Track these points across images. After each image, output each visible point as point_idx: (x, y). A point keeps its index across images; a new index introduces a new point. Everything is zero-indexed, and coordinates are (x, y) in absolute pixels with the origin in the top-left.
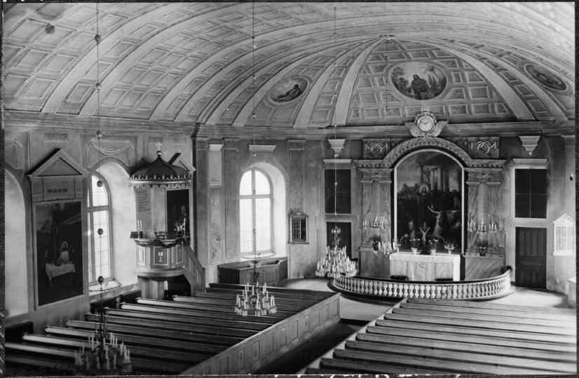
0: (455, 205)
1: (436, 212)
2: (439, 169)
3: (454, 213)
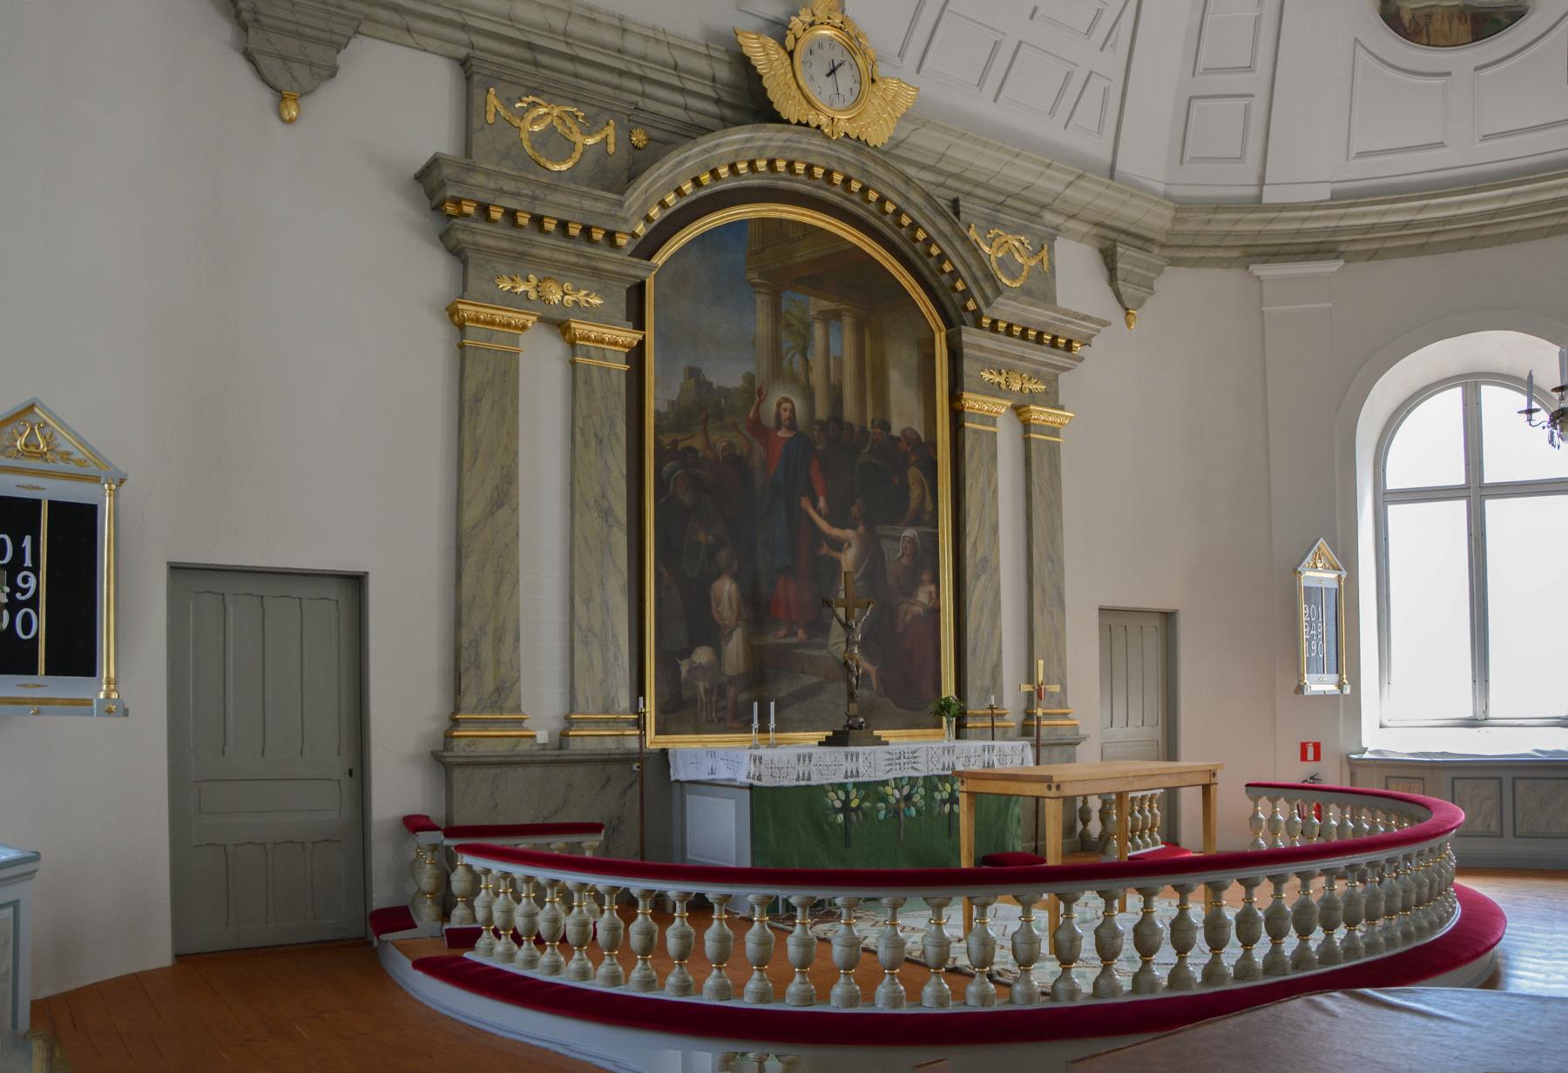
0: (913, 503)
1: (836, 532)
2: (848, 321)
3: (912, 540)
